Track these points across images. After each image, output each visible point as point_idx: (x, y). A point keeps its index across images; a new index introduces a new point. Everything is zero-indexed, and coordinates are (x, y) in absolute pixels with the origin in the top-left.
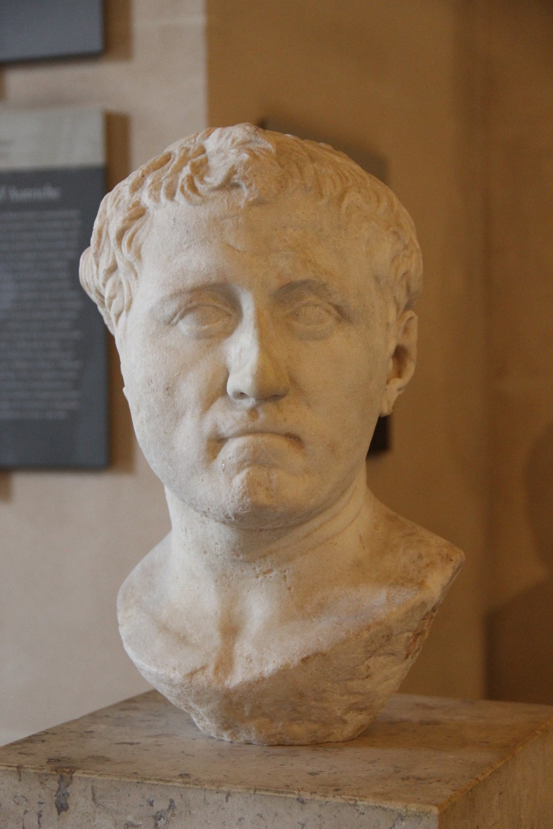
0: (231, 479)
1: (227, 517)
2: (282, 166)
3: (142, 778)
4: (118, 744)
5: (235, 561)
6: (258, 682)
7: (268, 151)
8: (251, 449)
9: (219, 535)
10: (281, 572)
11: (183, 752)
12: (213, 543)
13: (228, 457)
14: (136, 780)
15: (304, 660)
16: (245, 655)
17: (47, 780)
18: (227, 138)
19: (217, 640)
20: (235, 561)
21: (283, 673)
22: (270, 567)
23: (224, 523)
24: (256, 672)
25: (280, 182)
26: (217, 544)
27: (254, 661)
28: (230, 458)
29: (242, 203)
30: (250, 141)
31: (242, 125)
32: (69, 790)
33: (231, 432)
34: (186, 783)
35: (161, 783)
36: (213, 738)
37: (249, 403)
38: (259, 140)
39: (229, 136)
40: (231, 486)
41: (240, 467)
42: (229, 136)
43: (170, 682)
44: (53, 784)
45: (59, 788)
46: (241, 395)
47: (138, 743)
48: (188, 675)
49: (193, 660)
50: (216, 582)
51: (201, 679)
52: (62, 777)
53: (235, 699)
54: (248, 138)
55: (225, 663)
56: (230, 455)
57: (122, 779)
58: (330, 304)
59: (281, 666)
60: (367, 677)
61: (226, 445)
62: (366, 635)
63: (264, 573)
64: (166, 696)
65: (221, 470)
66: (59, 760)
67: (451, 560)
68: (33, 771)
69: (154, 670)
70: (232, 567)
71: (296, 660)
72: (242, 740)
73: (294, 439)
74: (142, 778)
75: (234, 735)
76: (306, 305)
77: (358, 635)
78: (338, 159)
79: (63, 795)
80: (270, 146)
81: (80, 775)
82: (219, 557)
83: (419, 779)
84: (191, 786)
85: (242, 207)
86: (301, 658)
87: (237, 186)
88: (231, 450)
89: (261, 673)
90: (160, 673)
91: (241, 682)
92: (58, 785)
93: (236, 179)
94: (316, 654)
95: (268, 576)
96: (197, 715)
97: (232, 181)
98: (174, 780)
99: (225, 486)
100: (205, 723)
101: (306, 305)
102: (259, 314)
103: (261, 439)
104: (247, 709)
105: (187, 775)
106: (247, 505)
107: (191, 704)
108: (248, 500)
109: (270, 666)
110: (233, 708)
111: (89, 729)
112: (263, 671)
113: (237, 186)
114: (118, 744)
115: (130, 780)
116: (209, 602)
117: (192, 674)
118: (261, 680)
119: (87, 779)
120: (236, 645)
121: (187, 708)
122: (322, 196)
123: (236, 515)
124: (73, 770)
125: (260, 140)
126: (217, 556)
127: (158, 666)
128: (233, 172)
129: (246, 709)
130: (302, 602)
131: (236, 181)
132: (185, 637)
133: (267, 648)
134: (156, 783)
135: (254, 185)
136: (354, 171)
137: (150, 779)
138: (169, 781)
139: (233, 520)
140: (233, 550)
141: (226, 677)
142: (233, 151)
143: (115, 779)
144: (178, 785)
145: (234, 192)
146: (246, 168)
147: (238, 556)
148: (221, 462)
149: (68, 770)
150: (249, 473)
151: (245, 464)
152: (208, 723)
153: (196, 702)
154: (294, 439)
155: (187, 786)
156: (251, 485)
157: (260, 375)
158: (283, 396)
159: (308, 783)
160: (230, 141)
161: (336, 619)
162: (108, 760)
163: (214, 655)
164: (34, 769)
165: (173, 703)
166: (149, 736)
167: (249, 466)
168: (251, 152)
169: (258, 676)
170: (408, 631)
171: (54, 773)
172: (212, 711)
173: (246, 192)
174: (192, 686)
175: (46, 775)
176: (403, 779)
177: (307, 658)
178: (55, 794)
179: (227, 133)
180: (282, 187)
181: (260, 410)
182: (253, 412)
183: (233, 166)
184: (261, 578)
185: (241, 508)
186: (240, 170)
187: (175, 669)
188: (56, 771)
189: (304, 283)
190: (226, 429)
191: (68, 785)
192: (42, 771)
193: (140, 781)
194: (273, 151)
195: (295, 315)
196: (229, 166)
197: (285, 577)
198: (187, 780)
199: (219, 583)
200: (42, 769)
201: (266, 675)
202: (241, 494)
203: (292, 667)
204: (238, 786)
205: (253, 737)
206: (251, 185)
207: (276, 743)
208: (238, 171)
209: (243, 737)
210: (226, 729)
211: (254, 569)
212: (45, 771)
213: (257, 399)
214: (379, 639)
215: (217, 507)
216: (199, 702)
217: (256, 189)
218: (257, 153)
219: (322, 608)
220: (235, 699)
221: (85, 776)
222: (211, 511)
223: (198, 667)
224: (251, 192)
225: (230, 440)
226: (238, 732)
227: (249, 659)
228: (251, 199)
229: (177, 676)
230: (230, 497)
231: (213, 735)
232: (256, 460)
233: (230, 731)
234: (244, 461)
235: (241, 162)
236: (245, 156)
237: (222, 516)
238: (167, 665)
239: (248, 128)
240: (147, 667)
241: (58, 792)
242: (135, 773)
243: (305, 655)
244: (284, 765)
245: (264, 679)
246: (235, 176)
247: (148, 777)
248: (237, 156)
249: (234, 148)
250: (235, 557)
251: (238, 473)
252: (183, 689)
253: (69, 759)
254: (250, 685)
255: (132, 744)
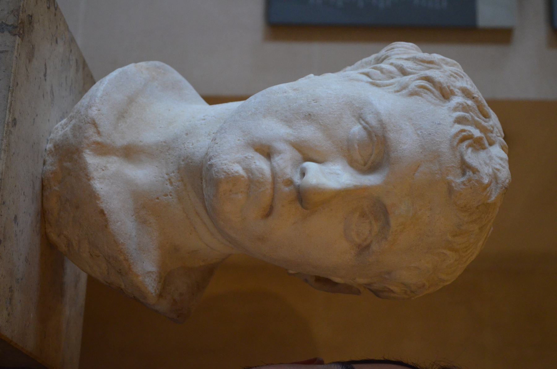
0: (239, 162)
1: (210, 159)
2: (477, 208)
3: (13, 90)
4: (45, 65)
5: (180, 157)
6: (86, 175)
7: (489, 197)
8: (262, 180)
9: (198, 146)
10: (171, 192)
11: (37, 115)
12: (193, 141)
13: (256, 161)
14: (11, 86)
15: (102, 212)
16: (108, 165)
17: (14, 15)
18: (500, 164)
19: (120, 142)
20: (180, 157)
21: (93, 196)
22: (174, 184)
23: (207, 154)
24: (95, 174)
25: (465, 206)
26: (193, 145)
27: (102, 172)
28: (255, 163)
29: (450, 178)
30: (497, 183)
31: (510, 176)
32: (6, 33)
33: (274, 164)
34: (8, 125)
35: (9, 105)
36: (50, 135)
37: (297, 179)
38: (498, 190)
39: (502, 166)
40: (234, 163)
41: (248, 170)
42: (502, 166)
43: (89, 107)
44: (11, 20)
45: (7, 25)
46: (303, 174)
47: (45, 80)
48: (94, 121)
49: (105, 125)
50: (165, 142)
51: (91, 131)
52: (16, 27)
53: (75, 156)
54: (500, 182)
55: (103, 149)
56: (258, 163)
57: (12, 74)
58: (371, 241)
59: (98, 194)
60: (91, 255)
61: (266, 159)
62: (121, 258)
63: (170, 180)
64: (80, 101)
65: (246, 155)
66: (30, 23)
67: (178, 317)
68: (21, 5)
69: (99, 94)
70: (175, 154)
71: (103, 206)
72: (47, 158)
73: (269, 212)
74: (13, 90)
75: (50, 153)
76: (370, 222)
77: (121, 252)
78: (480, 243)
79: (3, 28)
80: (493, 198)
81: (17, 42)
82: (183, 146)
83: (11, 299)
84: (5, 129)
85: (448, 178)
86: (104, 209)
87: (464, 174)
88: (261, 164)
89: (93, 178)
90: (97, 99)
91: (87, 162)
92: (10, 24)
93: (469, 173)
94: (106, 220)
95: (168, 182)
96: (66, 124)
97: (468, 170)
98: (11, 115)
99: (233, 159)
100: (59, 129)
101: (370, 222)
102: (365, 189)
103: (269, 186)
104: (68, 164)
105: (15, 124)
106: (219, 175)
107: (74, 121)
108: (222, 176)
109: (99, 186)
110: (68, 154)
111: (59, 40)
112: (95, 179)
113: (464, 174)
114: (45, 65)
115: (11, 81)
116: (150, 137)
117: (94, 124)
118: (88, 178)
119: (14, 47)
120: (115, 158)
121: (71, 117)
122: (454, 236)
123: (211, 165)
124: (22, 36)
125: (498, 191)
126: (183, 144)
127: (102, 97)
128: (475, 171)
129: (69, 164)
130: (146, 206)
131: (468, 173)
132: (124, 117)
133: (112, 181)
134: (9, 101)
135: (464, 187)
136: (472, 255)
137: (12, 96)
138: (10, 111)
139: (209, 163)
140: (187, 158)
141: (91, 150)
142: (491, 170)
143: (13, 69)
144: (7, 119)
145: (459, 171)
146: (477, 181)
147: (183, 160)
148: (252, 155)
149: (21, 32)
150: (243, 177)
151: (250, 175)
152: (60, 133)
153: (74, 126)
154: (269, 212)
155: (6, 126)
156: (234, 179)
157: (318, 191)
158: (302, 206)
159: (7, 218)
160: (498, 167)
161: (134, 234)
162: (30, 61)
163: (108, 141)
164: (23, 5)
165: (76, 106)
166: (52, 87)
167: (249, 177)
168: (489, 184)
169: (91, 176)
170: (125, 286)
171: (20, 21)
172: (67, 138)
173: (459, 180)
174: (86, 123)
175: (18, 15)
176: (10, 288)
177: (104, 214)
178: (4, 22)
179: (504, 165)
180: (462, 208)
181: (291, 188)
182: (290, 182)
183: (479, 171)
184: (166, 176)
185: (217, 170)
186: (476, 177)
187: (99, 110)
188: (20, 23)
189: (387, 223)
190: (278, 160)
191: (10, 32)
192: (21, 12)
193: (11, 89)
194: (489, 201)
195: (363, 215)
196: (479, 167)
197: (166, 195)
198: (10, 125)
199: (164, 144)
200: (22, 12)
201: (92, 182)
202: (227, 171)
203: (98, 202)
204: (4, 166)
205: (48, 167)
206: (464, 185)
207: (44, 184)
208: (475, 175)
209: (50, 160)
210: (55, 147)
211: (173, 172)
212: (21, 15)
213: (299, 186)
214: (118, 263)
215: (218, 151)
216: (74, 128)
217: (461, 189)
218: (488, 189)
219: (142, 221)
220: (75, 156)
221: (16, 45)
222: (216, 145)
223: (100, 130)
224: (459, 184)
225: (269, 163)
226: (53, 156)
227: (104, 168)
228: (453, 185)
229: (94, 112)
230: (225, 162)
231: (52, 136)
232: (252, 182)
233: (53, 149)
234: (252, 174)
235: (482, 178)
236: (486, 181)
237: (211, 154)
238: (103, 104)
239: (507, 181)
240: (102, 88)
241: (5, 24)
242: (17, 84)
243: (106, 212)
244: (24, 194)
245: (89, 180)
246: (471, 173)
247: (14, 95)
248: (486, 174)
249: (494, 172)
250: (183, 158)
251: (244, 169)
252: (84, 116)
253: (32, 31)
254: (85, 169)
255: (45, 75)
